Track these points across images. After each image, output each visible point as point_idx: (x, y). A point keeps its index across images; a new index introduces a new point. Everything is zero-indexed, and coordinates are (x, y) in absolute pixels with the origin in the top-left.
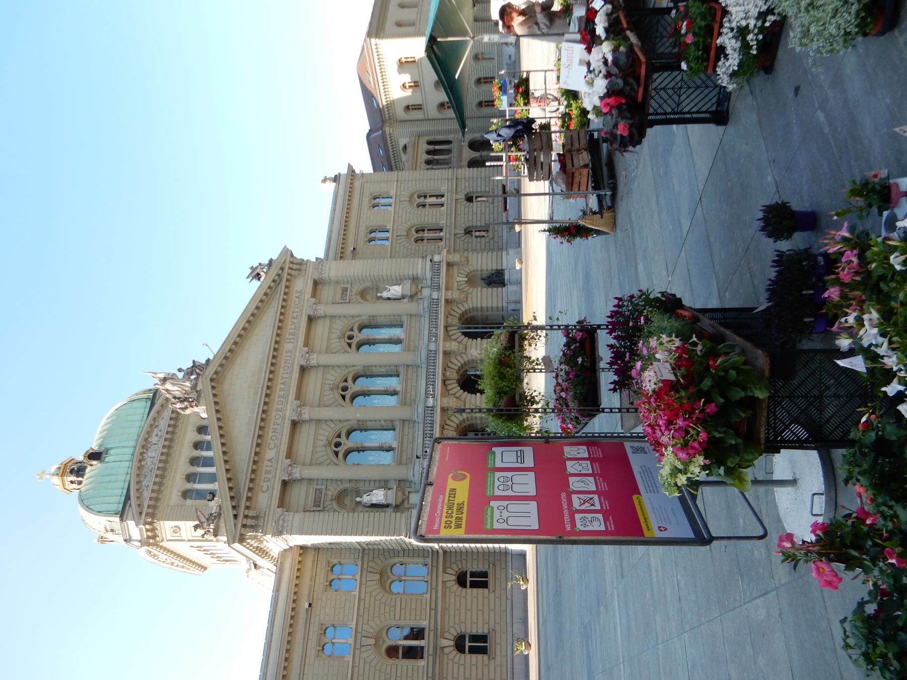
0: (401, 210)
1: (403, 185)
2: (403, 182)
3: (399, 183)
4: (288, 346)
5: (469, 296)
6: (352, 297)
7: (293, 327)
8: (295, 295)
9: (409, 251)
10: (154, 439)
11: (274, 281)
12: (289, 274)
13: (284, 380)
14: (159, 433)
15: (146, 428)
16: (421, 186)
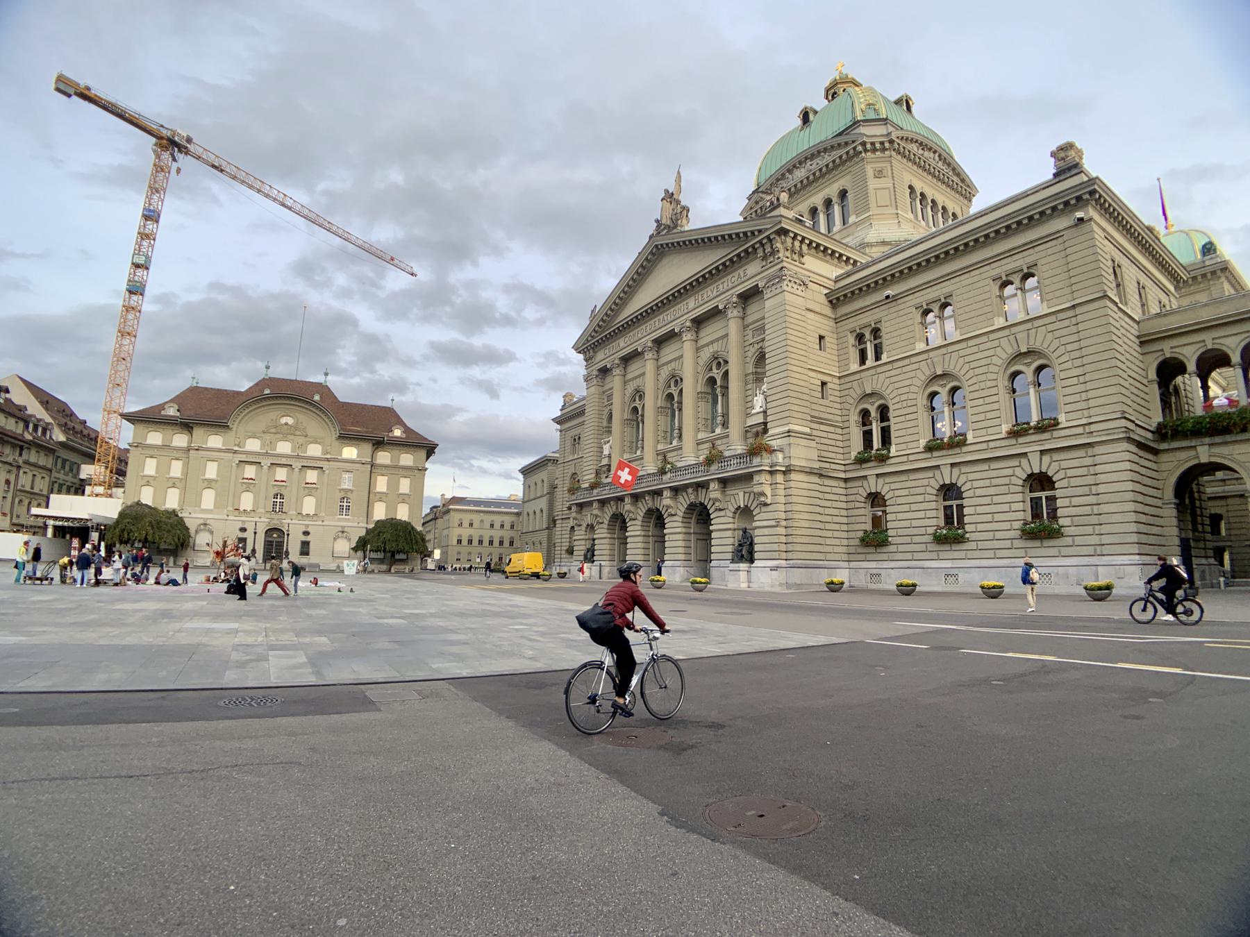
0: (996, 343)
1: (1066, 323)
2: (1074, 320)
3: (1071, 313)
4: (691, 303)
5: (722, 513)
6: (756, 345)
7: (709, 293)
8: (741, 271)
9: (906, 390)
10: (809, 163)
11: (745, 234)
12: (753, 246)
13: (666, 318)
14: (813, 166)
15: (814, 151)
16: (1069, 365)
